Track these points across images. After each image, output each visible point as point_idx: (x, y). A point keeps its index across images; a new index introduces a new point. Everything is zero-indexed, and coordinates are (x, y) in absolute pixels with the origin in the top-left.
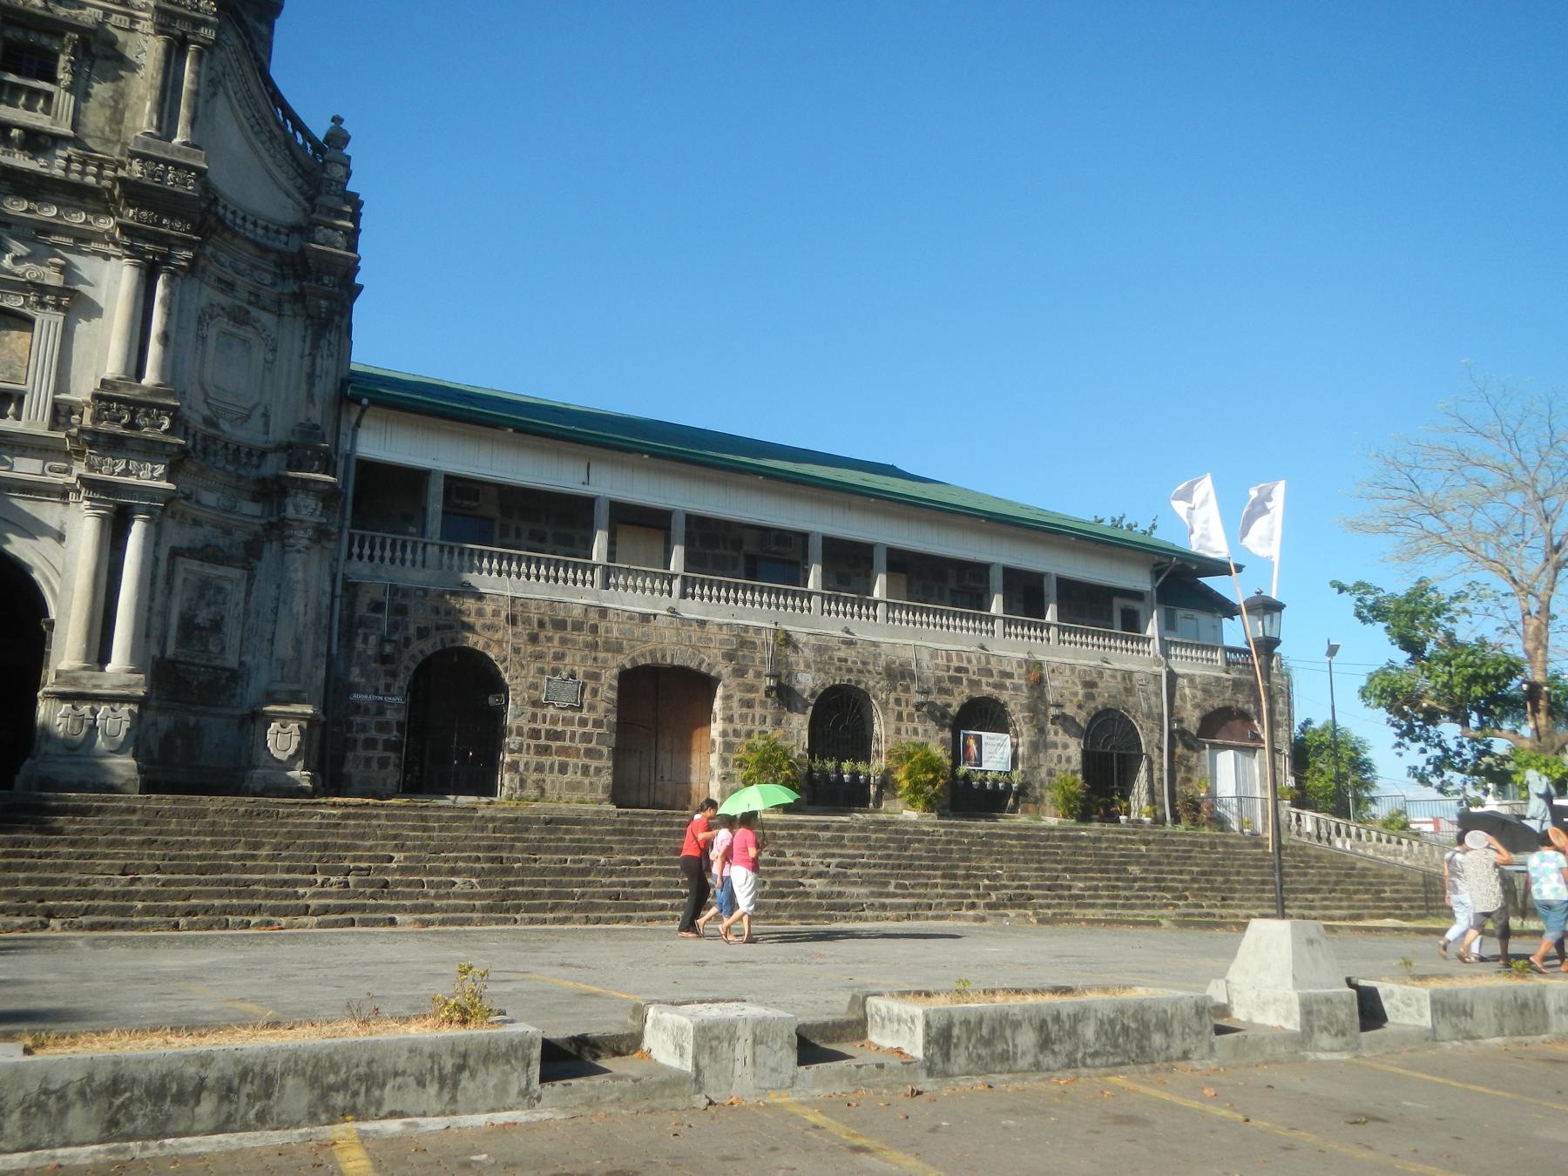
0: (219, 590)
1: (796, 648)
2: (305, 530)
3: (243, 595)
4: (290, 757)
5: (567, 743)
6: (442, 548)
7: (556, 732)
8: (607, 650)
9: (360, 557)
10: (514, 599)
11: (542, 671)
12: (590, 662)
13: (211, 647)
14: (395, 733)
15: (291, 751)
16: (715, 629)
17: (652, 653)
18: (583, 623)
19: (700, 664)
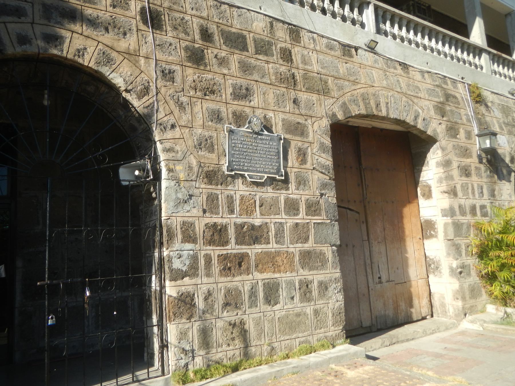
1: (487, 106)
5: (273, 246)
7: (253, 227)
8: (310, 90)
12: (289, 106)
16: (418, 76)
17: (365, 98)
18: (270, 44)
19: (416, 118)
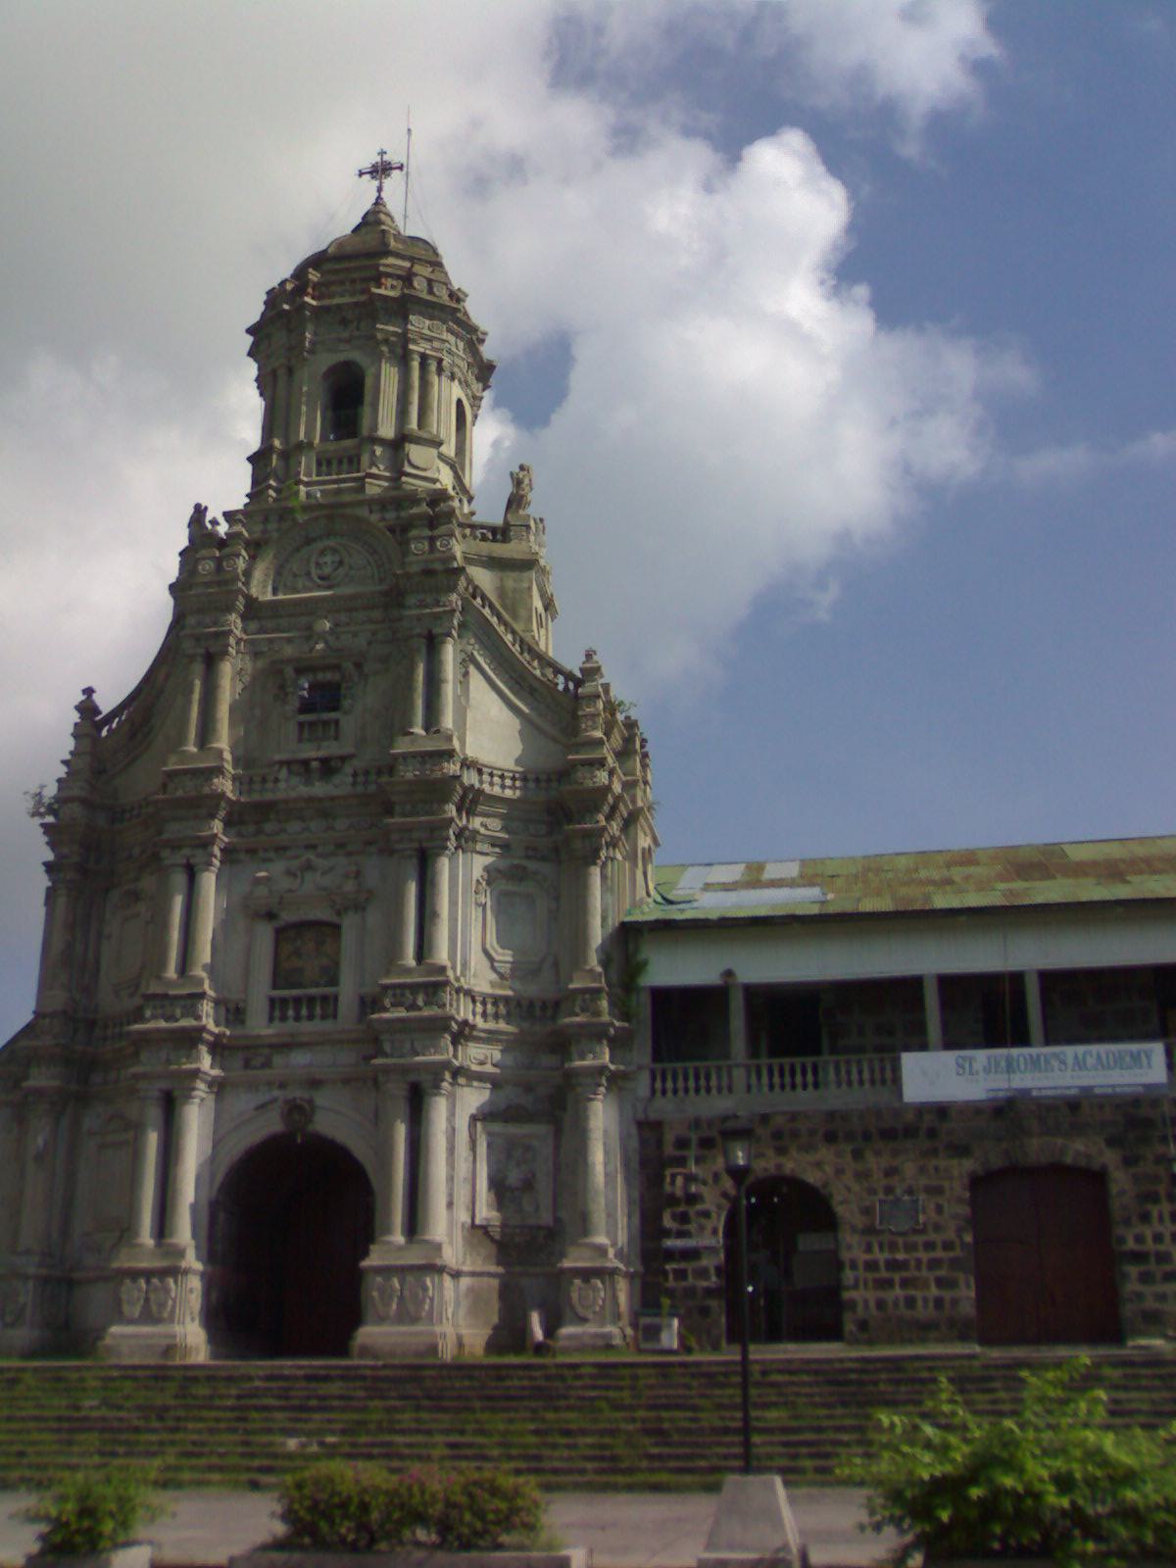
0: (528, 1148)
6: (748, 1068)
7: (896, 1261)
9: (664, 1092)
10: (831, 1115)
11: (872, 1191)
14: (714, 1279)
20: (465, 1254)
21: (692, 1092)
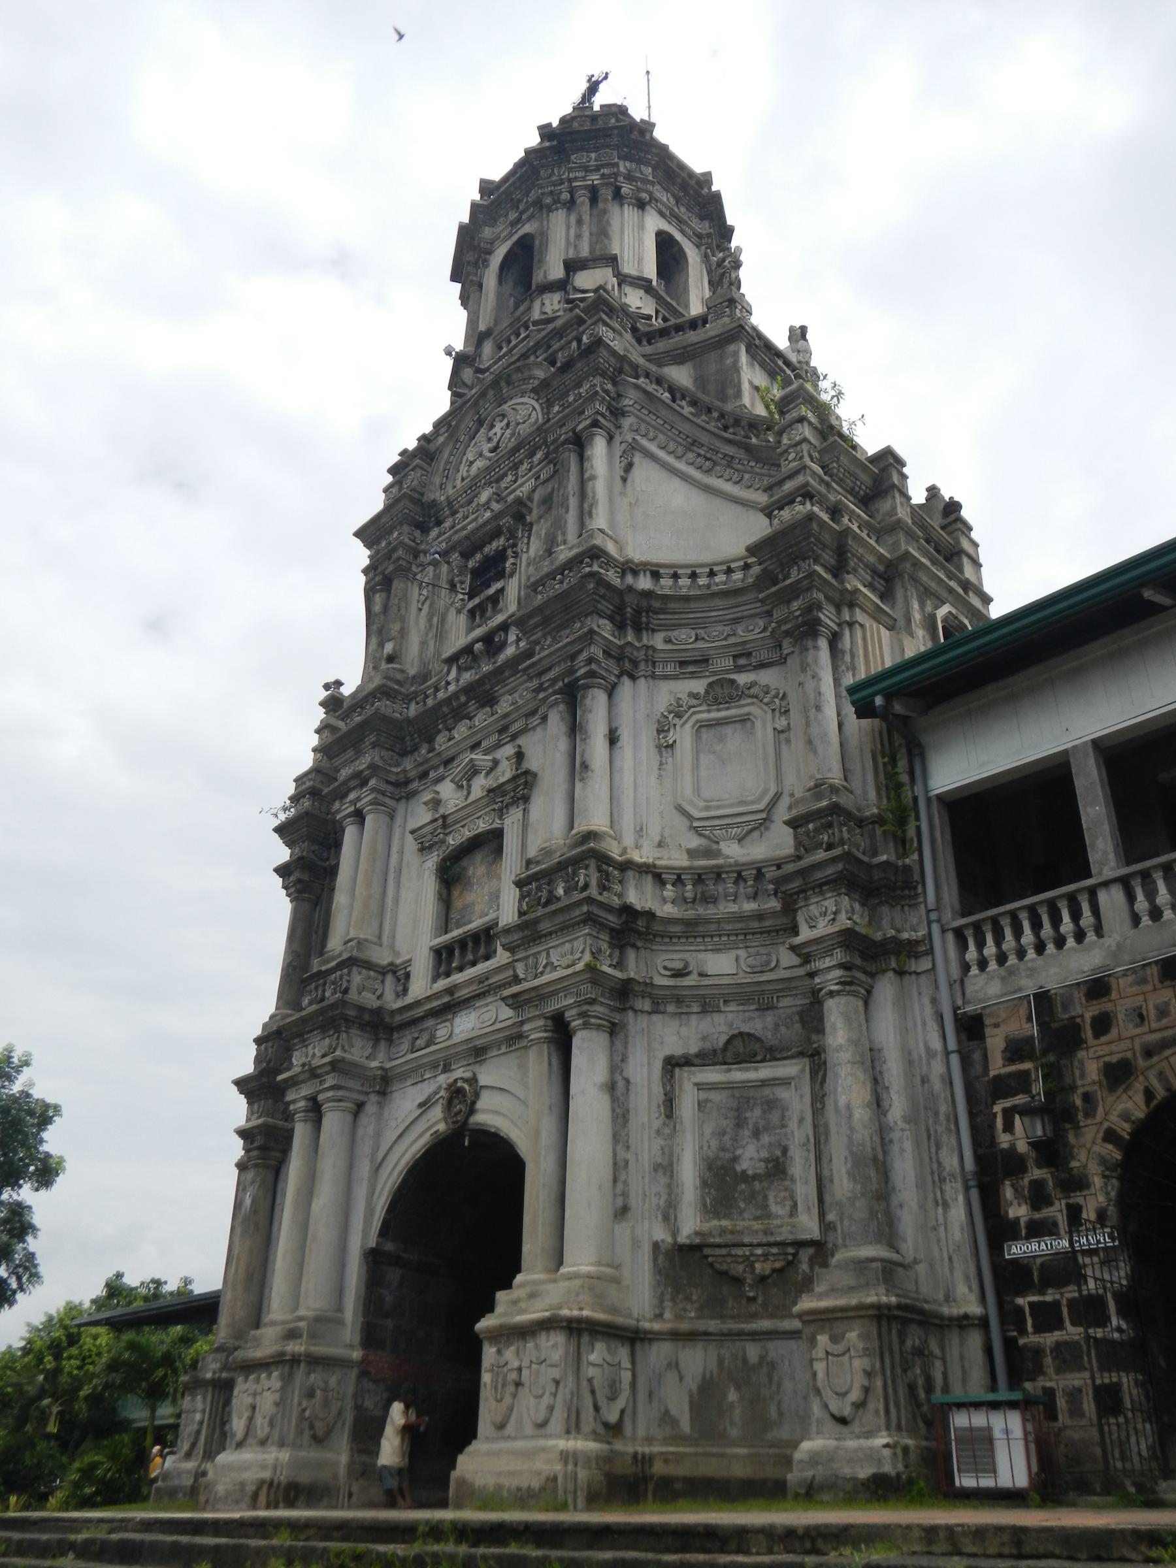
0: (771, 1105)
2: (828, 952)
3: (807, 1100)
4: (860, 1405)
6: (1125, 882)
13: (774, 1208)
15: (855, 1395)
20: (661, 1301)
21: (1031, 954)
